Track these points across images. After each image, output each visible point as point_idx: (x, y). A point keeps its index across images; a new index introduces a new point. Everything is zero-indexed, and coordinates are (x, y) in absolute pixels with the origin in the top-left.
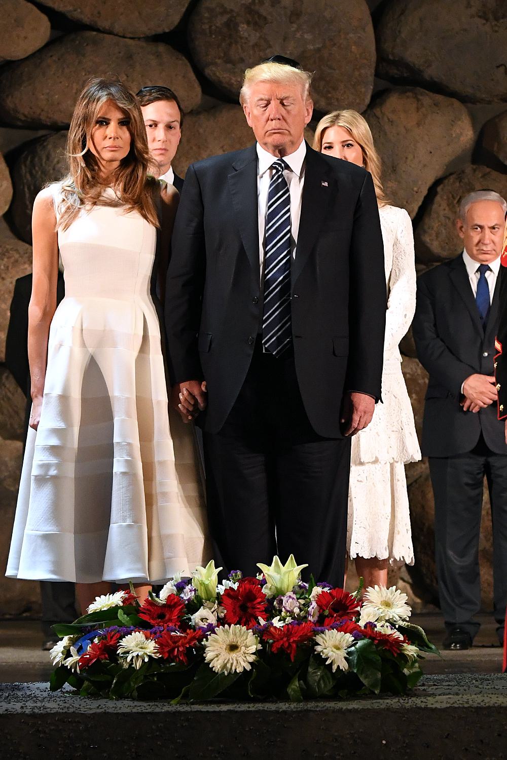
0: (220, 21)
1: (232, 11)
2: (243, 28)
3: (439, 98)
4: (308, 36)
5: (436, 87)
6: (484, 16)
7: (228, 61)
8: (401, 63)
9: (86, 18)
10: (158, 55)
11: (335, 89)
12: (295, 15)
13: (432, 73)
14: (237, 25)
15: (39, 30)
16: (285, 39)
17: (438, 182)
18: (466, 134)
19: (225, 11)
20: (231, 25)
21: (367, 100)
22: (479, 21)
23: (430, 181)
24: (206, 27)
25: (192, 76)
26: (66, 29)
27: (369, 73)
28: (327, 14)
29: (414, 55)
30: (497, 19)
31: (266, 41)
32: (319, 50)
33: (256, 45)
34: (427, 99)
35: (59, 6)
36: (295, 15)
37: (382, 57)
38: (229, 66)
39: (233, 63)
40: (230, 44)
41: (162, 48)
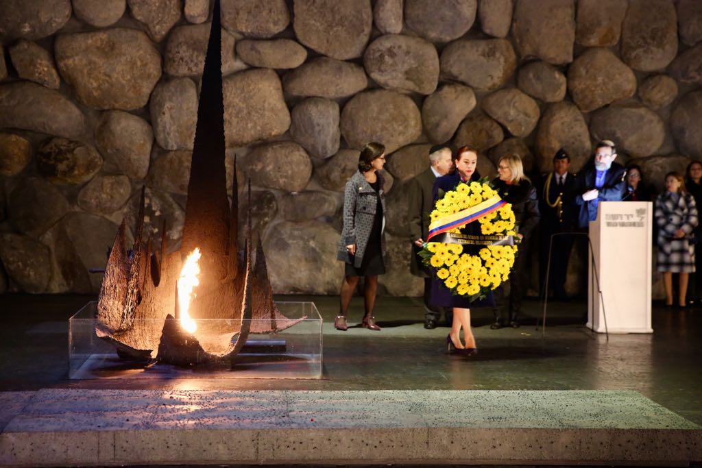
0: (377, 54)
1: (382, 50)
2: (386, 57)
3: (463, 87)
4: (413, 62)
5: (463, 83)
6: (484, 55)
7: (380, 70)
8: (451, 74)
9: (323, 52)
10: (352, 68)
11: (423, 83)
12: (408, 53)
13: (462, 78)
14: (384, 56)
15: (301, 57)
16: (404, 62)
17: (463, 122)
18: (473, 102)
19: (379, 51)
20: (382, 56)
21: (435, 88)
22: (482, 58)
23: (459, 121)
24: (372, 57)
25: (365, 76)
26: (314, 57)
27: (436, 77)
28: (421, 52)
29: (455, 70)
30: (489, 56)
31: (396, 63)
32: (417, 68)
33: (391, 65)
34: (460, 88)
35: (312, 47)
36: (408, 53)
37: (442, 72)
38: (380, 73)
39: (382, 72)
40: (381, 64)
41: (353, 65)
